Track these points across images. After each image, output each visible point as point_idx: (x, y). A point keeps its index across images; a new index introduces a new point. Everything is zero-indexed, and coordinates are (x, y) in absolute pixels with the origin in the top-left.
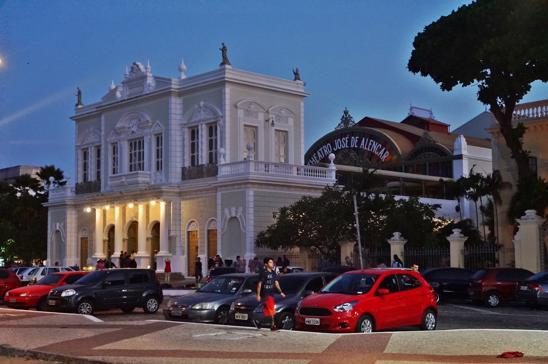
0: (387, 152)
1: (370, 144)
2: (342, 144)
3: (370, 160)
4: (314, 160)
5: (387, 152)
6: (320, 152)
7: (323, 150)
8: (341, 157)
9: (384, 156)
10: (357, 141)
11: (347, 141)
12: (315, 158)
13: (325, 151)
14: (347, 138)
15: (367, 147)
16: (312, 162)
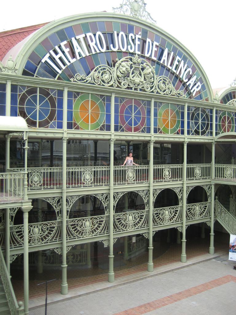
0: (199, 83)
1: (176, 63)
2: (128, 44)
3: (177, 89)
4: (61, 54)
5: (199, 83)
6: (78, 41)
7: (85, 38)
8: (129, 69)
9: (195, 87)
10: (155, 49)
11: (137, 42)
12: (67, 50)
13: (92, 45)
14: (137, 36)
15: (172, 64)
16: (57, 58)
